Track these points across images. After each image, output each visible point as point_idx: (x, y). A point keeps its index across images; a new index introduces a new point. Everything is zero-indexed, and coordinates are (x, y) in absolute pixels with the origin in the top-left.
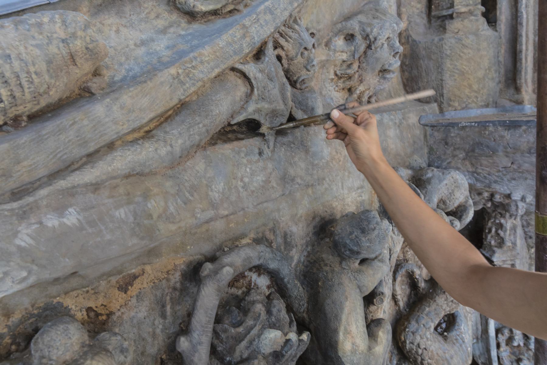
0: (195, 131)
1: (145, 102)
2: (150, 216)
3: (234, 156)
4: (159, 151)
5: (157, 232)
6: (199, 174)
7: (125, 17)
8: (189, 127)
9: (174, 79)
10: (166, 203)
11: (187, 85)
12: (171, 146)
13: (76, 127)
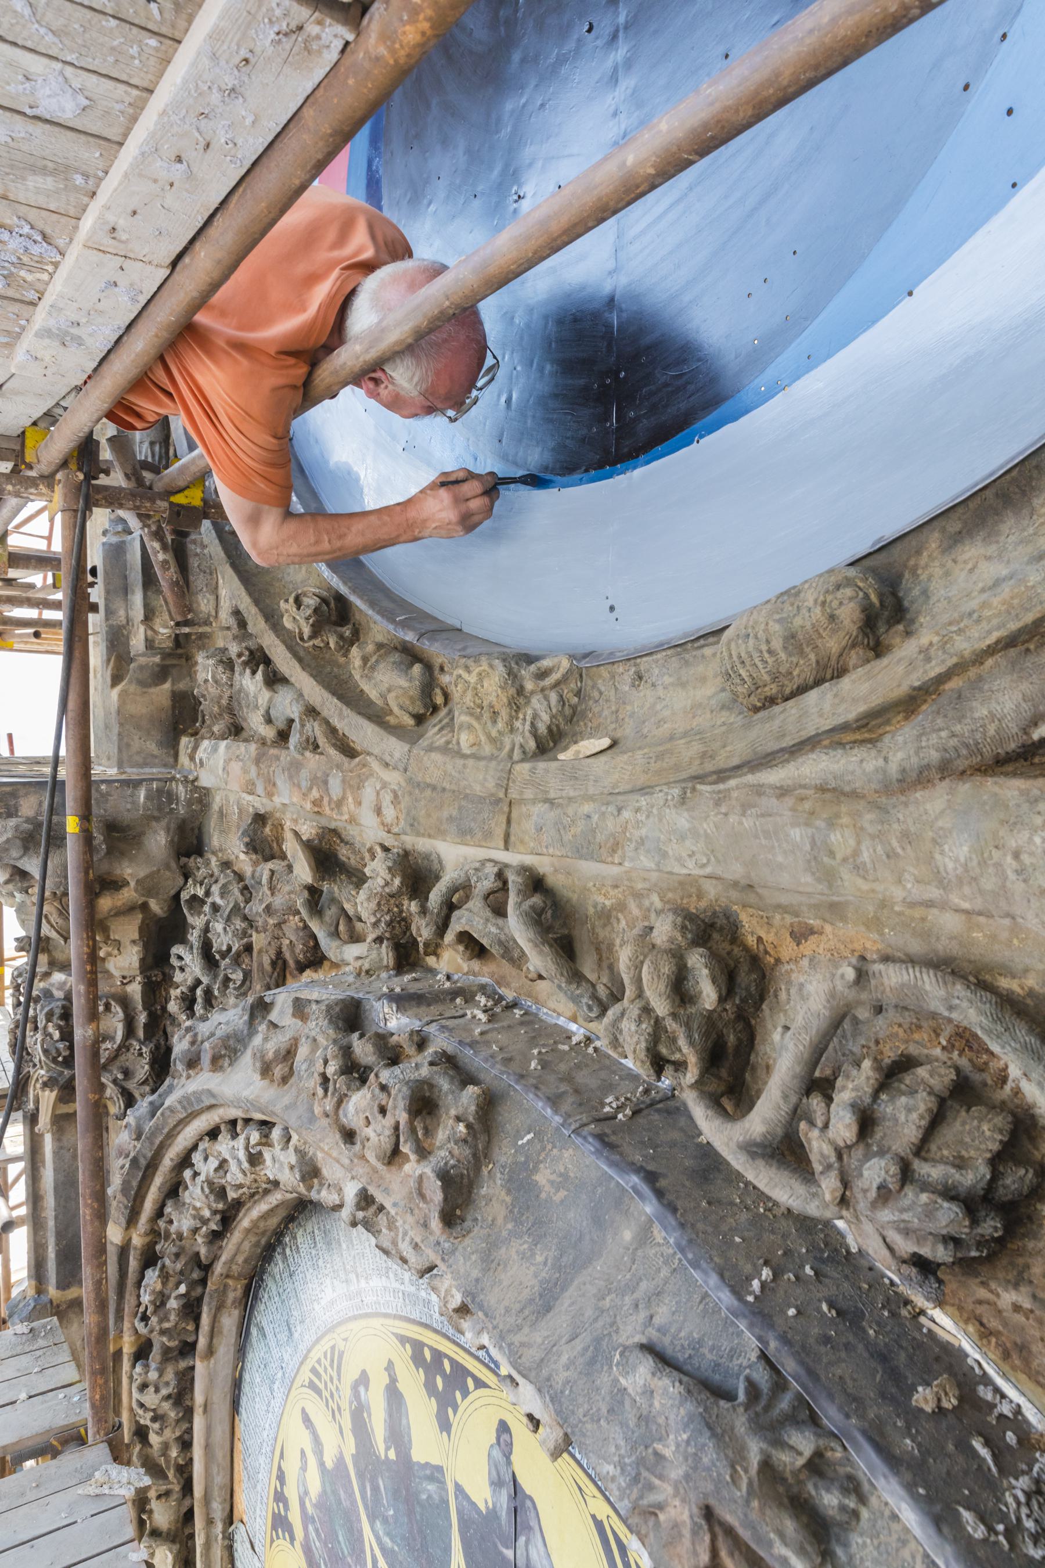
0: (931, 742)
1: (864, 688)
2: (832, 854)
3: (1018, 806)
4: (864, 764)
5: (839, 883)
6: (924, 817)
7: (997, 542)
8: (921, 735)
9: (920, 652)
10: (859, 843)
11: (934, 663)
12: (886, 759)
13: (782, 716)
